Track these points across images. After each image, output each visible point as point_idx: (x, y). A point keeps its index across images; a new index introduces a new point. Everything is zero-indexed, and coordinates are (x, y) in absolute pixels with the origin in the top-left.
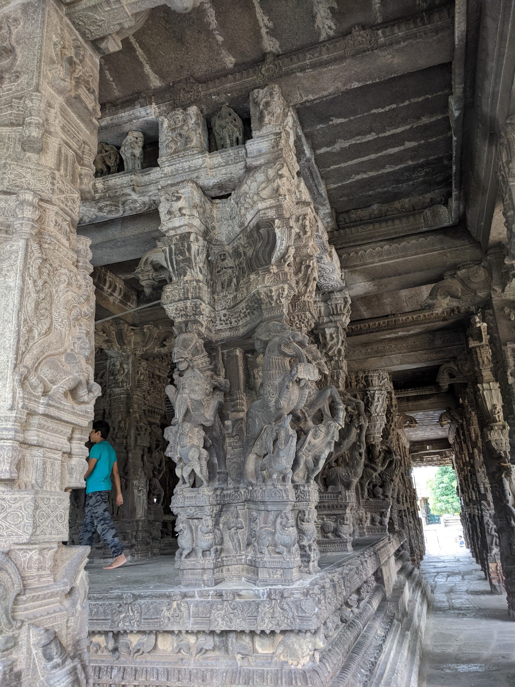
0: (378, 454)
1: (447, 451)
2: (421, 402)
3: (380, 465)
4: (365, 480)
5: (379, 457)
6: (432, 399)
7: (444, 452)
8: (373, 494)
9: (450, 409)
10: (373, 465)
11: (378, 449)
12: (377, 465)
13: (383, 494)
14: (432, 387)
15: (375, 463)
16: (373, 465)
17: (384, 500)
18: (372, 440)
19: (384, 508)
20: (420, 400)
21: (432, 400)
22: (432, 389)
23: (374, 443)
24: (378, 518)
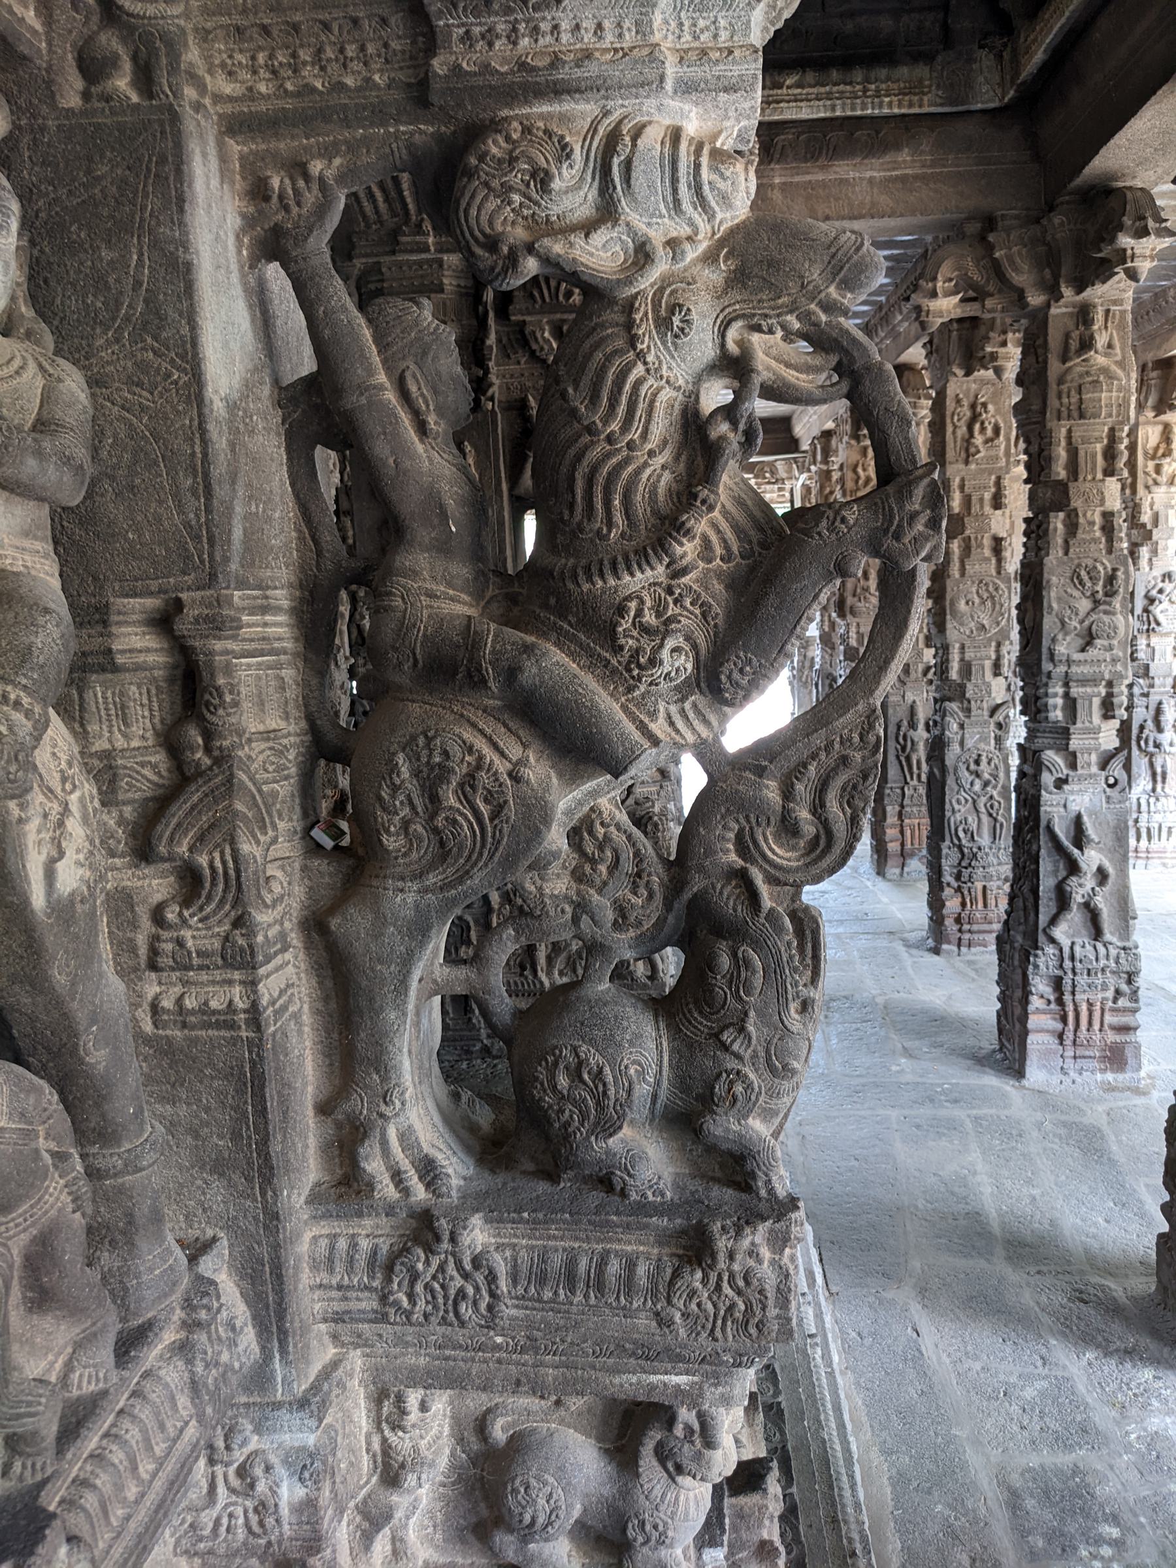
0: (656, 468)
1: (779, 461)
2: (845, 169)
3: (676, 662)
4: (403, 899)
5: (668, 525)
6: (905, 155)
7: (772, 464)
8: (524, 1126)
9: (990, 222)
10: (556, 663)
11: (673, 372)
12: (628, 672)
13: (688, 1114)
14: (922, 71)
15: (596, 630)
16: (556, 663)
17: (695, 1248)
18: (572, 192)
19: (675, 1358)
20: (837, 152)
21: (906, 161)
22: (913, 89)
23: (599, 254)
24: (573, 1470)
